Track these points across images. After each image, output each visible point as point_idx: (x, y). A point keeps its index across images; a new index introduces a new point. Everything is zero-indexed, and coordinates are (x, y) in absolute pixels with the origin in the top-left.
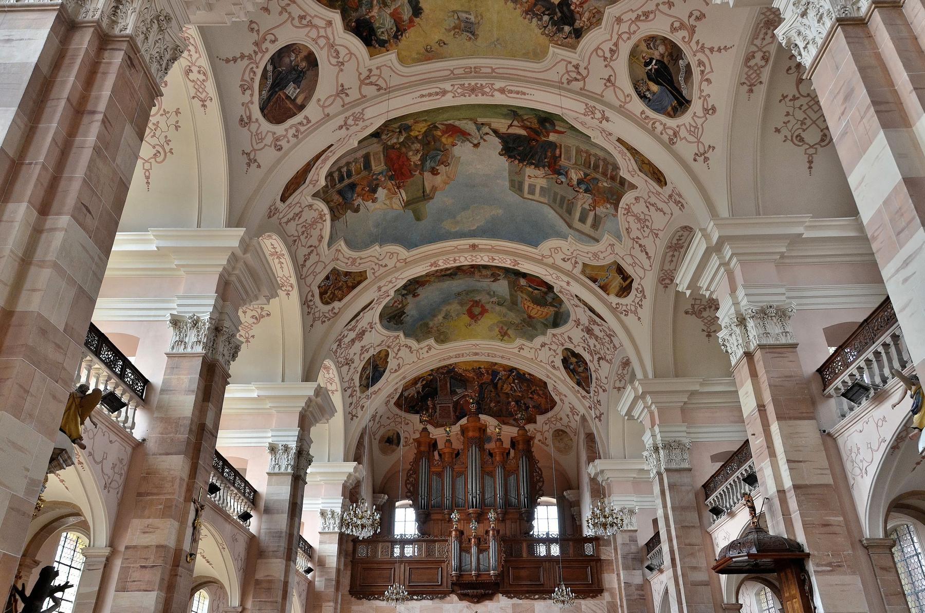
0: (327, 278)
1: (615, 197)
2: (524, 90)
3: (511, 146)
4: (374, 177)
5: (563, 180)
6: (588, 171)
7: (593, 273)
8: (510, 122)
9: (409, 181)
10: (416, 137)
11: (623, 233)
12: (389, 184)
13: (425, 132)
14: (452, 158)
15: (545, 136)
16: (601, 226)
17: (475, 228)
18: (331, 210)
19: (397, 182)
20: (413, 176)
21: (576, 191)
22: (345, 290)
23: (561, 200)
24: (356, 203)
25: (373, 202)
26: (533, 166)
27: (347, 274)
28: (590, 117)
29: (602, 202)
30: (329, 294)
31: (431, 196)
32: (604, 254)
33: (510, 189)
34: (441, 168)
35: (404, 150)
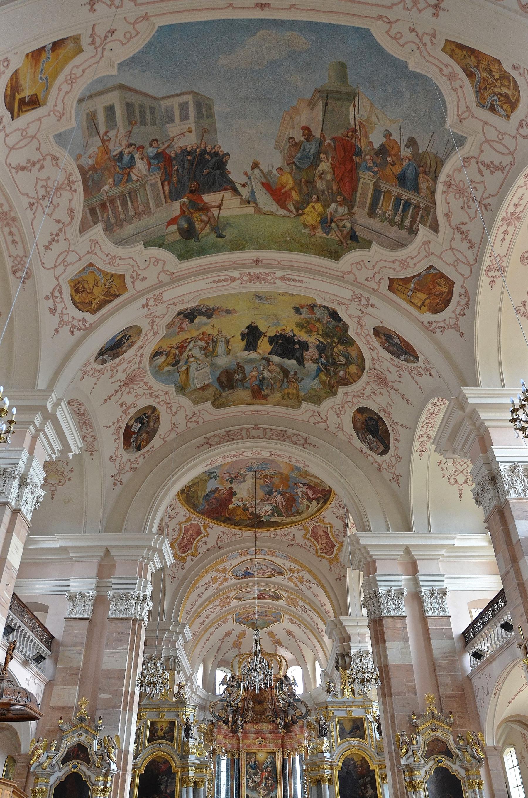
0: (492, 108)
1: (90, 183)
2: (215, 285)
3: (218, 172)
4: (376, 169)
5: (150, 150)
6: (129, 186)
7: (62, 52)
8: (223, 213)
9: (338, 134)
10: (318, 200)
11: (57, 150)
12: (362, 145)
13: (308, 204)
14: (283, 150)
15: (184, 204)
16: (85, 126)
17: (261, 32)
18: (435, 179)
19: (353, 141)
20: (334, 139)
21: (130, 145)
22: (484, 64)
23: (145, 117)
24: (409, 151)
25: (390, 135)
26: (189, 149)
27: (470, 75)
28: (157, 294)
29: (99, 159)
30: (505, 90)
31: (318, 95)
32: (62, 93)
33: (212, 100)
34: (299, 137)
35: (335, 187)
